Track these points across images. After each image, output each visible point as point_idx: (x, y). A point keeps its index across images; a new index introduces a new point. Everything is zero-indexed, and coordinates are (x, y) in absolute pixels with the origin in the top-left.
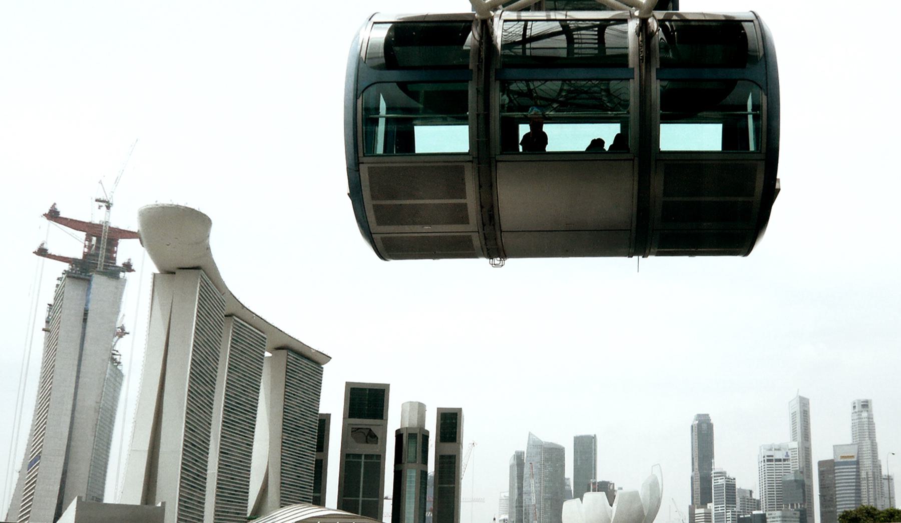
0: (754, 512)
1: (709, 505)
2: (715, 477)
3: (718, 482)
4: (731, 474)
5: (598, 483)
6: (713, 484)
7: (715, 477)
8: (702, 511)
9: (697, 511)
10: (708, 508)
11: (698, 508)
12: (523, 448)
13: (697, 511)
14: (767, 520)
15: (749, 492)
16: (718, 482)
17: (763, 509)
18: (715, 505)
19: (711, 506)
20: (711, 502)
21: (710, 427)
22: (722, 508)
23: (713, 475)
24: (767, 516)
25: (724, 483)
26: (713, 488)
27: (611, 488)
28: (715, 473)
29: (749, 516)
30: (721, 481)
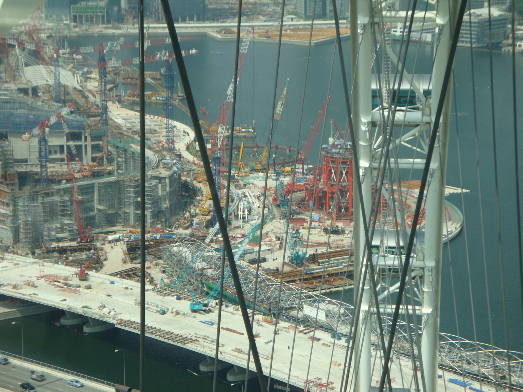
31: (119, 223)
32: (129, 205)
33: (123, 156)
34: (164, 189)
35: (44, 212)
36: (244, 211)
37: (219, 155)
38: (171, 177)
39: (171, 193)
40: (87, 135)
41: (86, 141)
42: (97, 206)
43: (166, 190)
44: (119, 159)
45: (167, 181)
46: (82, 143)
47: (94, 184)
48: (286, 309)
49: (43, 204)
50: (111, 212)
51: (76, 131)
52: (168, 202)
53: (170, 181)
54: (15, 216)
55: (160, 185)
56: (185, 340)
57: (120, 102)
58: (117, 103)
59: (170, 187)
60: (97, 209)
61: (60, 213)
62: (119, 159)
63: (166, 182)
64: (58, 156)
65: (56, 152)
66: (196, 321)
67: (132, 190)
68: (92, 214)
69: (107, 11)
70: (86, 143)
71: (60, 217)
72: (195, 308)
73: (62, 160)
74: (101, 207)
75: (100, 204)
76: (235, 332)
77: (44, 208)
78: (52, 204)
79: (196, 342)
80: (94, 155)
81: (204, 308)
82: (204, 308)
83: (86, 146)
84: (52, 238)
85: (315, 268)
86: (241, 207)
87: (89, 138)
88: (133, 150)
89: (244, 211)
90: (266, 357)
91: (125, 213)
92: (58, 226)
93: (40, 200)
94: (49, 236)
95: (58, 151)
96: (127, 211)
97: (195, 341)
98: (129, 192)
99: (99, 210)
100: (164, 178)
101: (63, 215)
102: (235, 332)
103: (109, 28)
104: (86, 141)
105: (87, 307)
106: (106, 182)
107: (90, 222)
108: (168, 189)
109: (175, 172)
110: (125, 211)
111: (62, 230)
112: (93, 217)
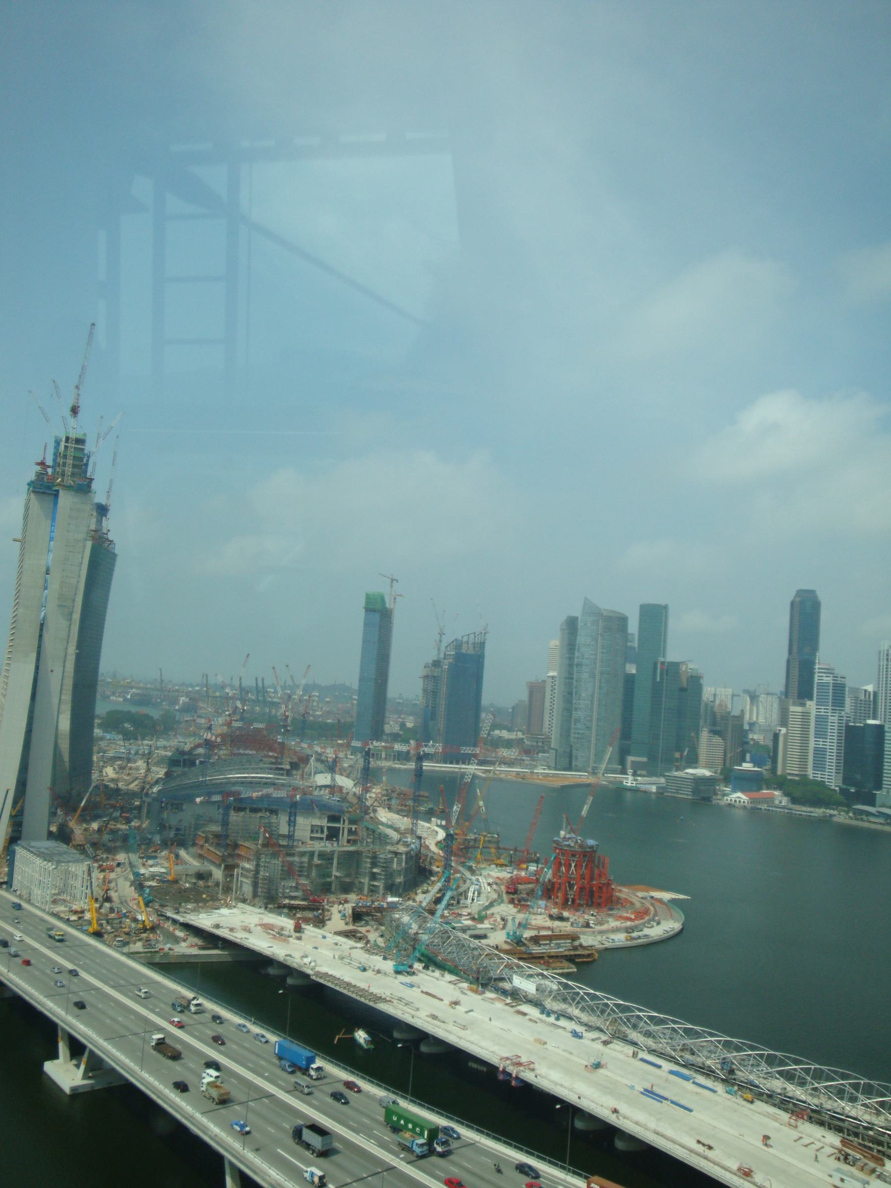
0: (871, 722)
1: (808, 703)
2: (819, 672)
3: (822, 680)
4: (839, 671)
5: (668, 663)
6: (816, 680)
7: (819, 672)
8: (799, 709)
9: (792, 708)
10: (808, 706)
11: (794, 704)
12: (577, 612)
13: (792, 708)
14: (886, 734)
15: (863, 692)
16: (822, 680)
17: (881, 718)
18: (817, 705)
19: (811, 705)
20: (811, 699)
21: (816, 606)
22: (827, 710)
23: (817, 670)
24: (886, 729)
25: (831, 682)
26: (815, 686)
27: (684, 668)
28: (819, 669)
29: (862, 725)
30: (828, 680)
31: (354, 892)
32: (365, 876)
33: (372, 837)
35: (282, 870)
36: (474, 893)
38: (407, 853)
39: (406, 869)
40: (345, 818)
41: (344, 824)
42: (335, 873)
43: (401, 866)
44: (369, 840)
45: (404, 857)
46: (340, 825)
48: (495, 980)
50: (347, 880)
51: (337, 814)
52: (402, 877)
53: (406, 858)
54: (257, 872)
55: (395, 859)
56: (380, 999)
57: (389, 808)
58: (386, 809)
59: (406, 863)
60: (335, 875)
61: (297, 873)
62: (369, 840)
63: (402, 858)
64: (319, 835)
65: (317, 832)
66: (397, 982)
67: (369, 860)
68: (328, 880)
70: (344, 826)
71: (296, 877)
72: (399, 970)
73: (321, 839)
74: (338, 874)
75: (337, 871)
76: (434, 996)
77: (283, 866)
78: (291, 864)
79: (389, 1003)
80: (350, 838)
81: (409, 970)
82: (409, 970)
83: (343, 828)
84: (286, 895)
85: (536, 950)
87: (347, 822)
88: (380, 831)
89: (474, 893)
90: (462, 1027)
91: (360, 882)
92: (294, 885)
94: (283, 893)
95: (319, 831)
96: (362, 881)
97: (388, 1001)
99: (336, 877)
100: (401, 854)
101: (300, 876)
102: (434, 996)
104: (344, 824)
105: (290, 956)
106: (345, 851)
107: (326, 889)
108: (403, 864)
109: (412, 850)
111: (296, 888)
112: (330, 884)
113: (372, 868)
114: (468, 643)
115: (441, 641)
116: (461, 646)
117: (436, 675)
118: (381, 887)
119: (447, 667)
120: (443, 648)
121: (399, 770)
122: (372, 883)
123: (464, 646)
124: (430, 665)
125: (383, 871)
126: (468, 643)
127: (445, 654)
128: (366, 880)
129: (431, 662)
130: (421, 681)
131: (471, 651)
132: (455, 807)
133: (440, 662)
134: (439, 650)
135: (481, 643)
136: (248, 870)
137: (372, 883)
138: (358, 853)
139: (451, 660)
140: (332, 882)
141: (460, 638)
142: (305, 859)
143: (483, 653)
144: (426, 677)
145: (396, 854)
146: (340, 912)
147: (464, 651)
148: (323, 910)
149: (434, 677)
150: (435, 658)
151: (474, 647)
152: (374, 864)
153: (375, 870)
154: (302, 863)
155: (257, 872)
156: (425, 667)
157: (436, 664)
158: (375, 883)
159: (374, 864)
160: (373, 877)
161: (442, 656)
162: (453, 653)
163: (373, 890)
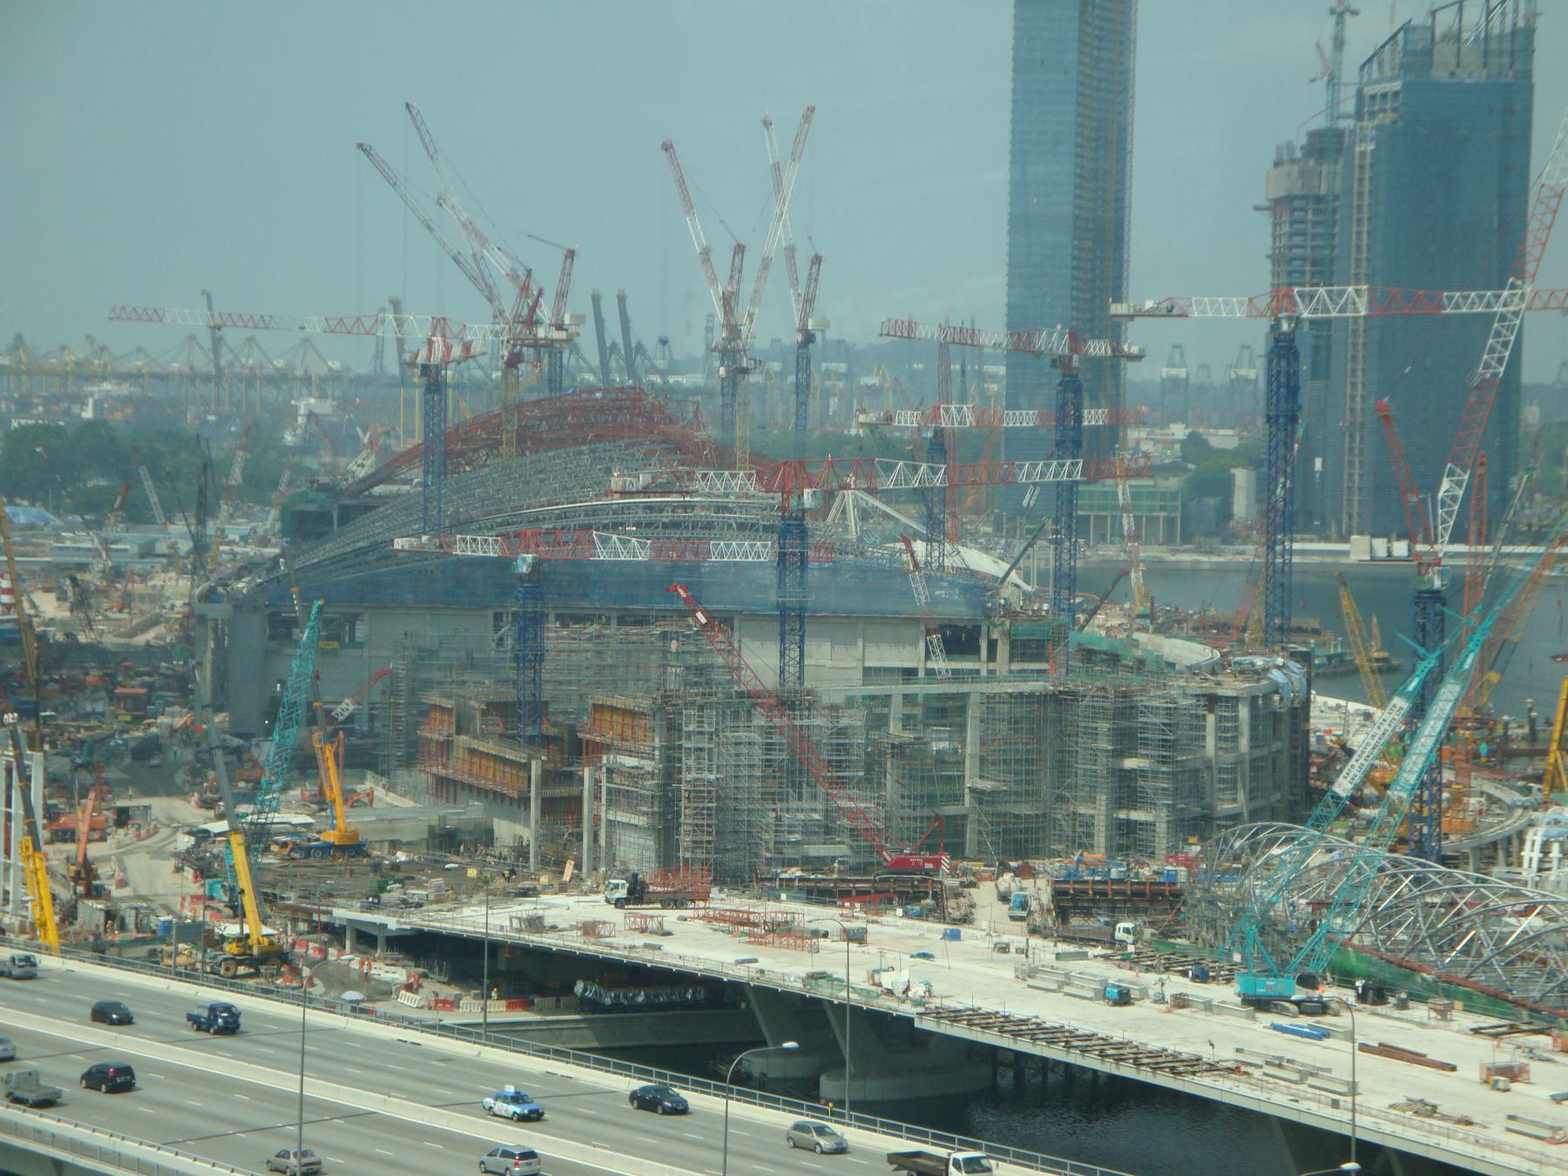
34: (1228, 736)
35: (768, 763)
37: (1437, 584)
39: (1255, 765)
40: (995, 635)
42: (972, 780)
43: (1236, 749)
45: (1244, 712)
47: (965, 696)
49: (767, 731)
50: (1025, 810)
53: (1254, 717)
54: (670, 773)
55: (1211, 719)
60: (972, 790)
63: (1236, 719)
66: (1258, 1027)
68: (950, 810)
69: (1184, 506)
71: (821, 790)
72: (1261, 991)
77: (769, 748)
84: (789, 852)
86: (1535, 837)
88: (1139, 653)
93: (759, 720)
98: (1094, 734)
99: (978, 794)
100: (1233, 701)
101: (841, 782)
103: (1186, 551)
108: (1244, 743)
110: (1074, 813)
111: (828, 831)
113: (1119, 754)
114: (1456, 37)
115: (1339, 43)
116: (1429, 53)
117: (1323, 191)
118: (1162, 828)
119: (1371, 147)
120: (1350, 73)
121: (1195, 571)
122: (1122, 815)
123: (1444, 55)
124: (1299, 154)
125: (1164, 760)
126: (1456, 37)
127: (1360, 95)
128: (1098, 810)
129: (1302, 140)
130: (1264, 222)
131: (1473, 73)
132: (1446, 484)
133: (1340, 134)
134: (1333, 81)
135: (1514, 32)
136: (635, 775)
137: (1122, 815)
138: (1060, 700)
139: (1389, 118)
140: (964, 817)
141: (1420, 19)
142: (853, 719)
143: (1527, 74)
144: (1281, 206)
145: (1212, 701)
146: (1004, 898)
147: (1440, 74)
148: (935, 896)
149: (1319, 199)
150: (1320, 123)
151: (1486, 54)
152: (1127, 741)
153: (1130, 763)
154: (842, 732)
155: (670, 773)
156: (1277, 164)
157: (1325, 145)
158: (1136, 815)
159: (1127, 741)
160: (1127, 790)
161: (1349, 106)
162: (1397, 85)
163: (1128, 838)
